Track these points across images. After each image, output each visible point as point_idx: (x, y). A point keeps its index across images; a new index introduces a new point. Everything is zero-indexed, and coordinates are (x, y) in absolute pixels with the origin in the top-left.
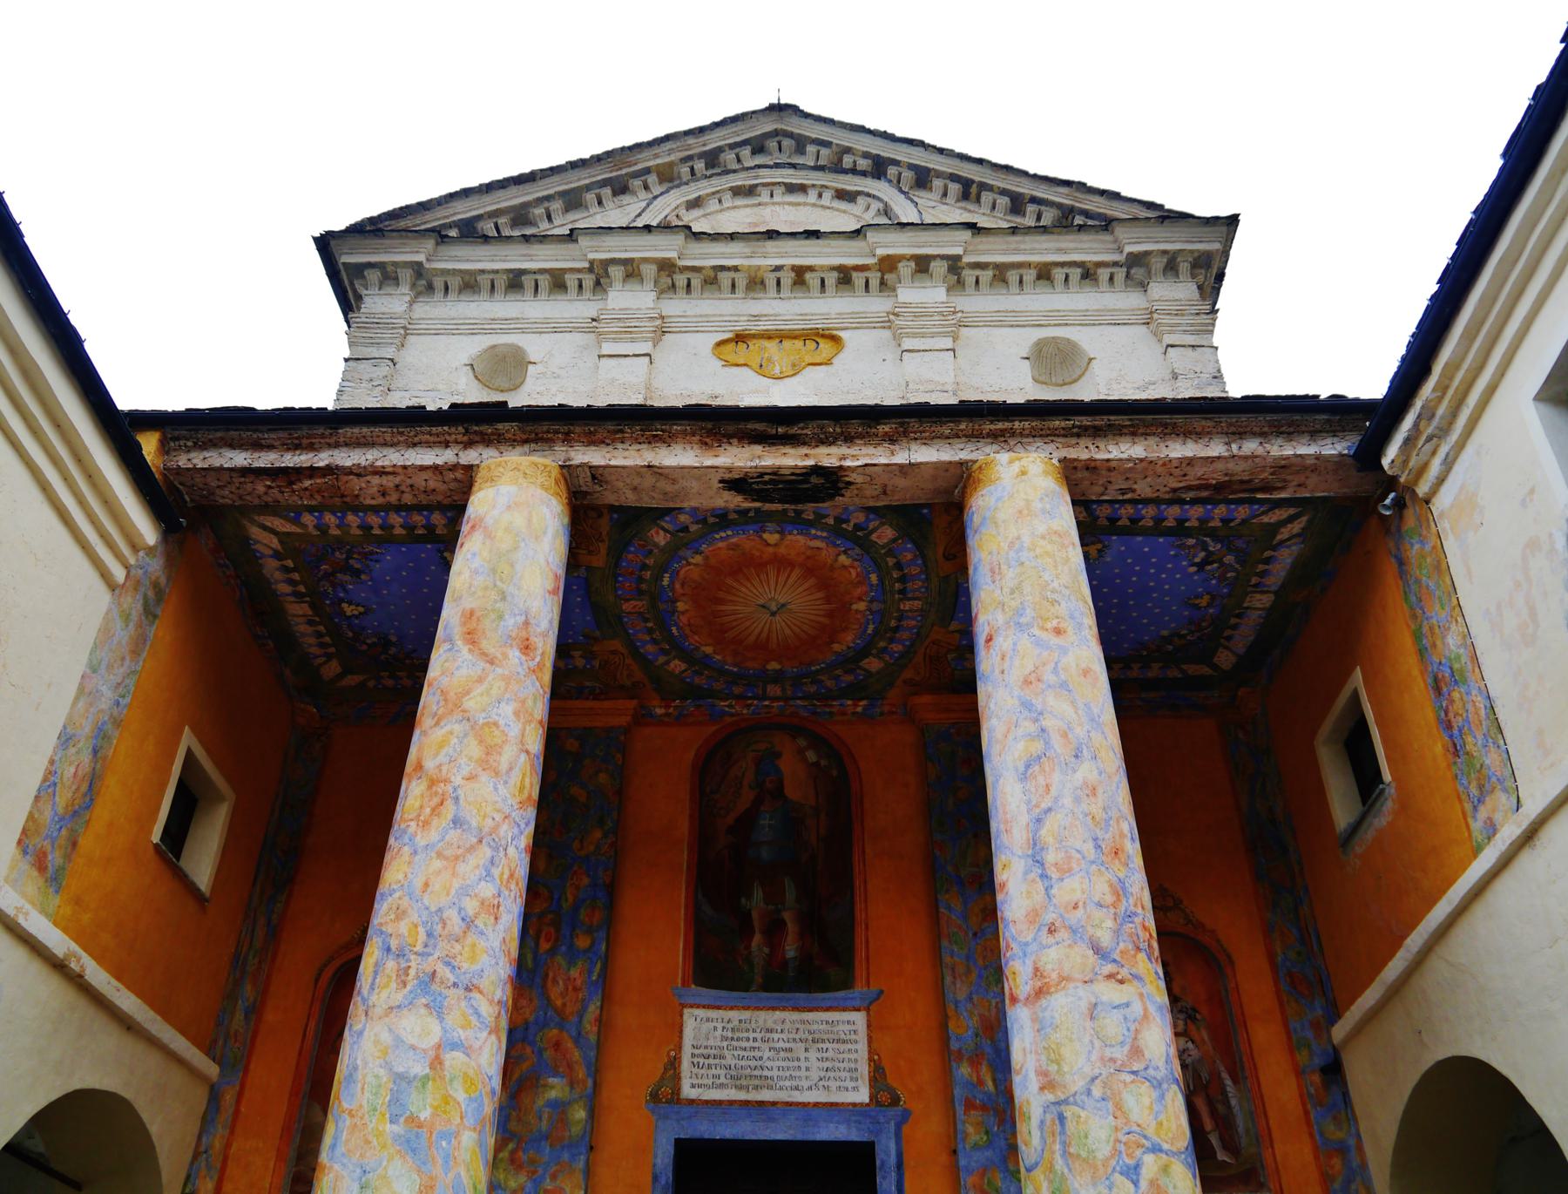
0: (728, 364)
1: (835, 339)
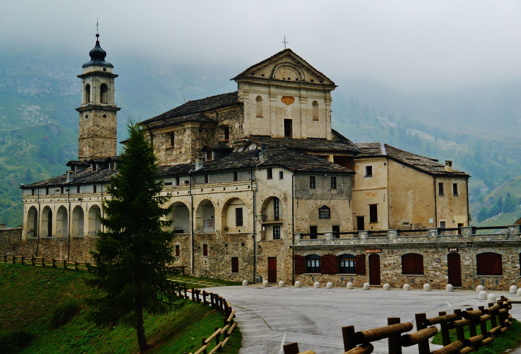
0: (283, 102)
1: (294, 99)
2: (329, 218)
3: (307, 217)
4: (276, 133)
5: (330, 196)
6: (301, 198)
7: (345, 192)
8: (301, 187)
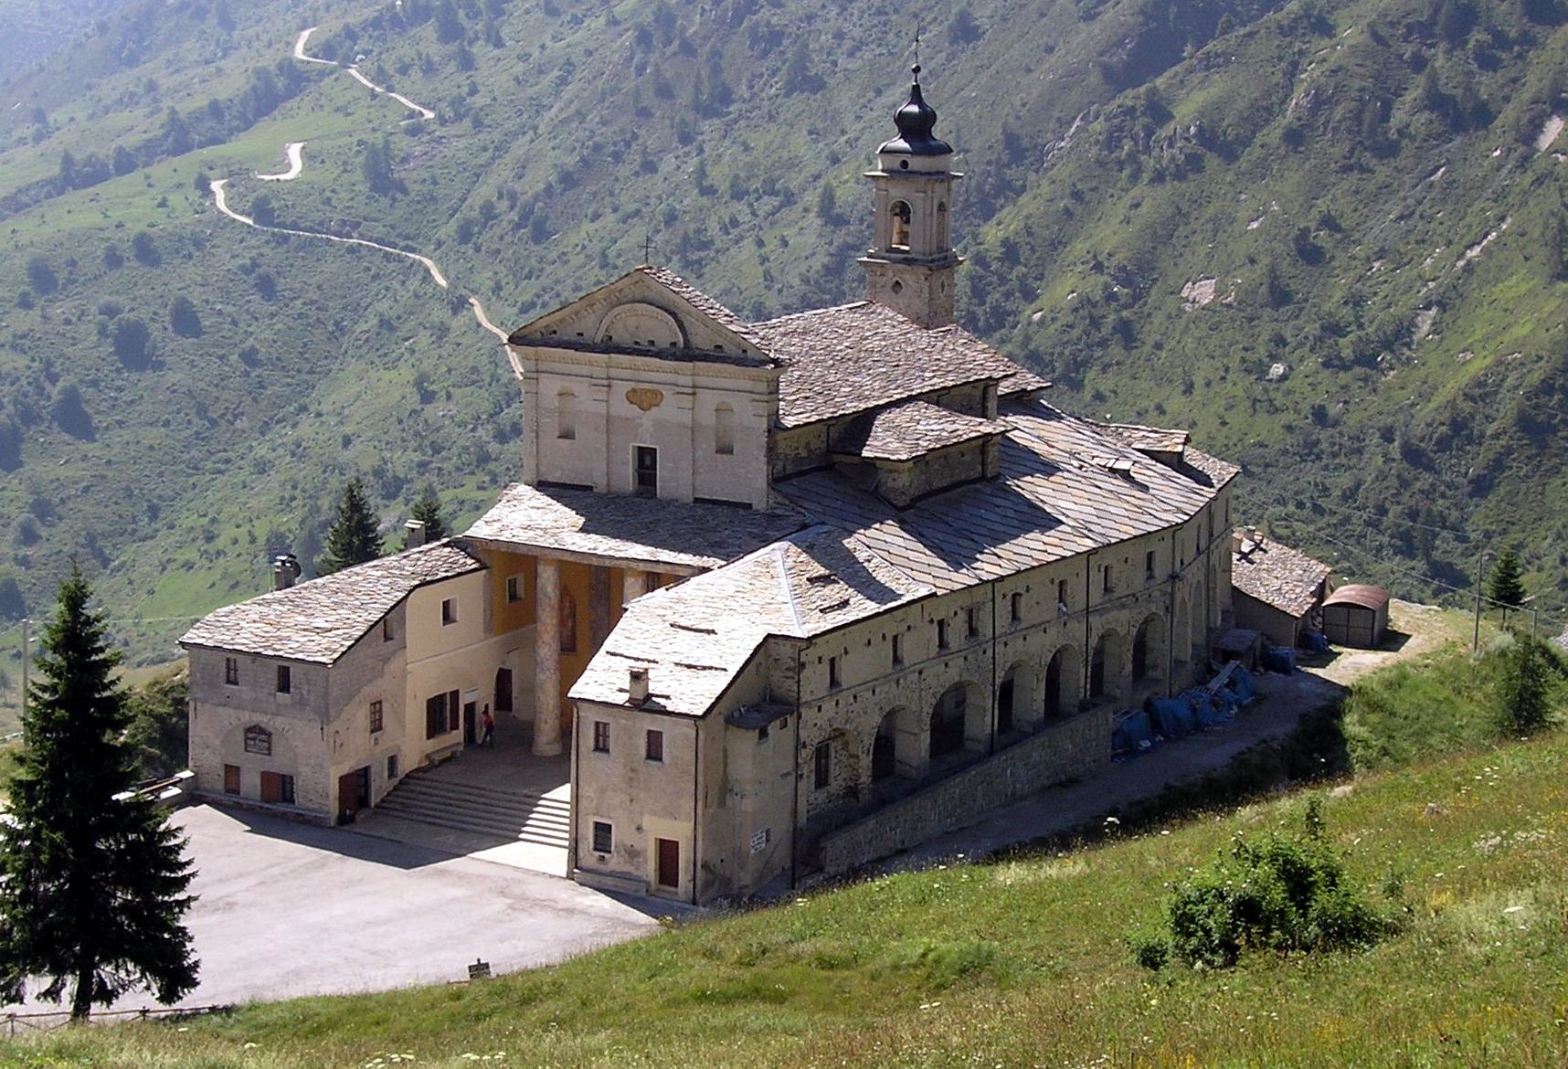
2: (269, 754)
3: (217, 742)
4: (605, 482)
5: (273, 707)
6: (205, 701)
7: (312, 704)
8: (202, 678)
